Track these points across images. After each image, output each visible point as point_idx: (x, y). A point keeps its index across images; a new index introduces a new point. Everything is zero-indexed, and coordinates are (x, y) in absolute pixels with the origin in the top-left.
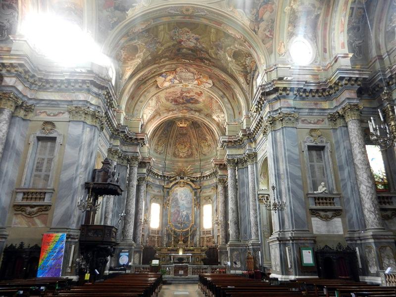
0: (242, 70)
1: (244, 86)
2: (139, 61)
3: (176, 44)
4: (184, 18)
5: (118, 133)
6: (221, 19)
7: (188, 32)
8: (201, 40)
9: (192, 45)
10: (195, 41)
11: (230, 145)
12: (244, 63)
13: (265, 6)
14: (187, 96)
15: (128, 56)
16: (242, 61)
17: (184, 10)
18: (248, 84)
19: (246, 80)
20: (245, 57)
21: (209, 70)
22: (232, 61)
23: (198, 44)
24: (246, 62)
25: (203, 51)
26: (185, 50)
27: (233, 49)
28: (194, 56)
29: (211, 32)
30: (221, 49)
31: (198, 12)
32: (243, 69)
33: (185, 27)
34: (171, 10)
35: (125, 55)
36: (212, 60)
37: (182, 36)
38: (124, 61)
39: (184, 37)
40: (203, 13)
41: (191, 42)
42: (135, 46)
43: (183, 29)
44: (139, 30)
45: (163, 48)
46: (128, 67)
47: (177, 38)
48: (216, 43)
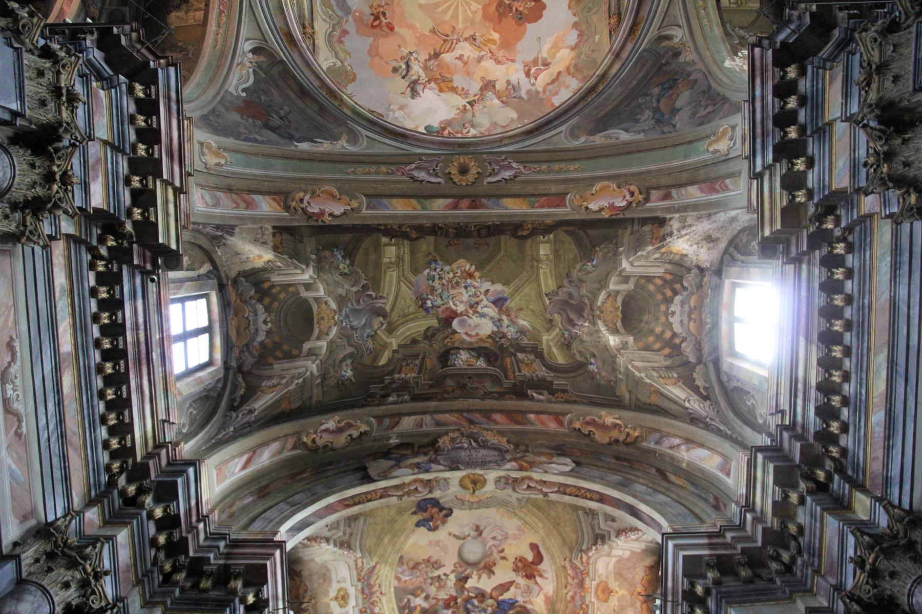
0: (667, 363)
1: (695, 405)
2: (313, 367)
3: (438, 330)
4: (455, 207)
5: (141, 491)
6: (560, 171)
7: (471, 276)
8: (512, 304)
9: (486, 328)
10: (492, 311)
11: (730, 583)
12: (668, 334)
13: (670, 92)
14: (481, 595)
15: (276, 339)
16: (658, 329)
17: (454, 171)
18: (706, 398)
19: (695, 389)
20: (663, 308)
21: (552, 426)
22: (625, 345)
23: (506, 322)
24: (670, 325)
25: (522, 350)
26: (464, 355)
27: (618, 292)
28: (496, 380)
29: (539, 261)
30: (581, 315)
31: (493, 173)
32: (668, 356)
33: (463, 258)
34: (416, 168)
35: (268, 332)
36: (558, 382)
37: (454, 292)
38: (261, 355)
39: (459, 301)
40: (507, 174)
41: (483, 315)
42: (305, 301)
43: (455, 265)
44: (322, 213)
45: (394, 343)
46: (269, 378)
47: (439, 302)
48: (562, 296)
